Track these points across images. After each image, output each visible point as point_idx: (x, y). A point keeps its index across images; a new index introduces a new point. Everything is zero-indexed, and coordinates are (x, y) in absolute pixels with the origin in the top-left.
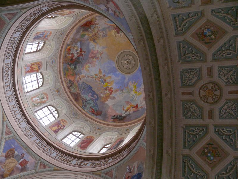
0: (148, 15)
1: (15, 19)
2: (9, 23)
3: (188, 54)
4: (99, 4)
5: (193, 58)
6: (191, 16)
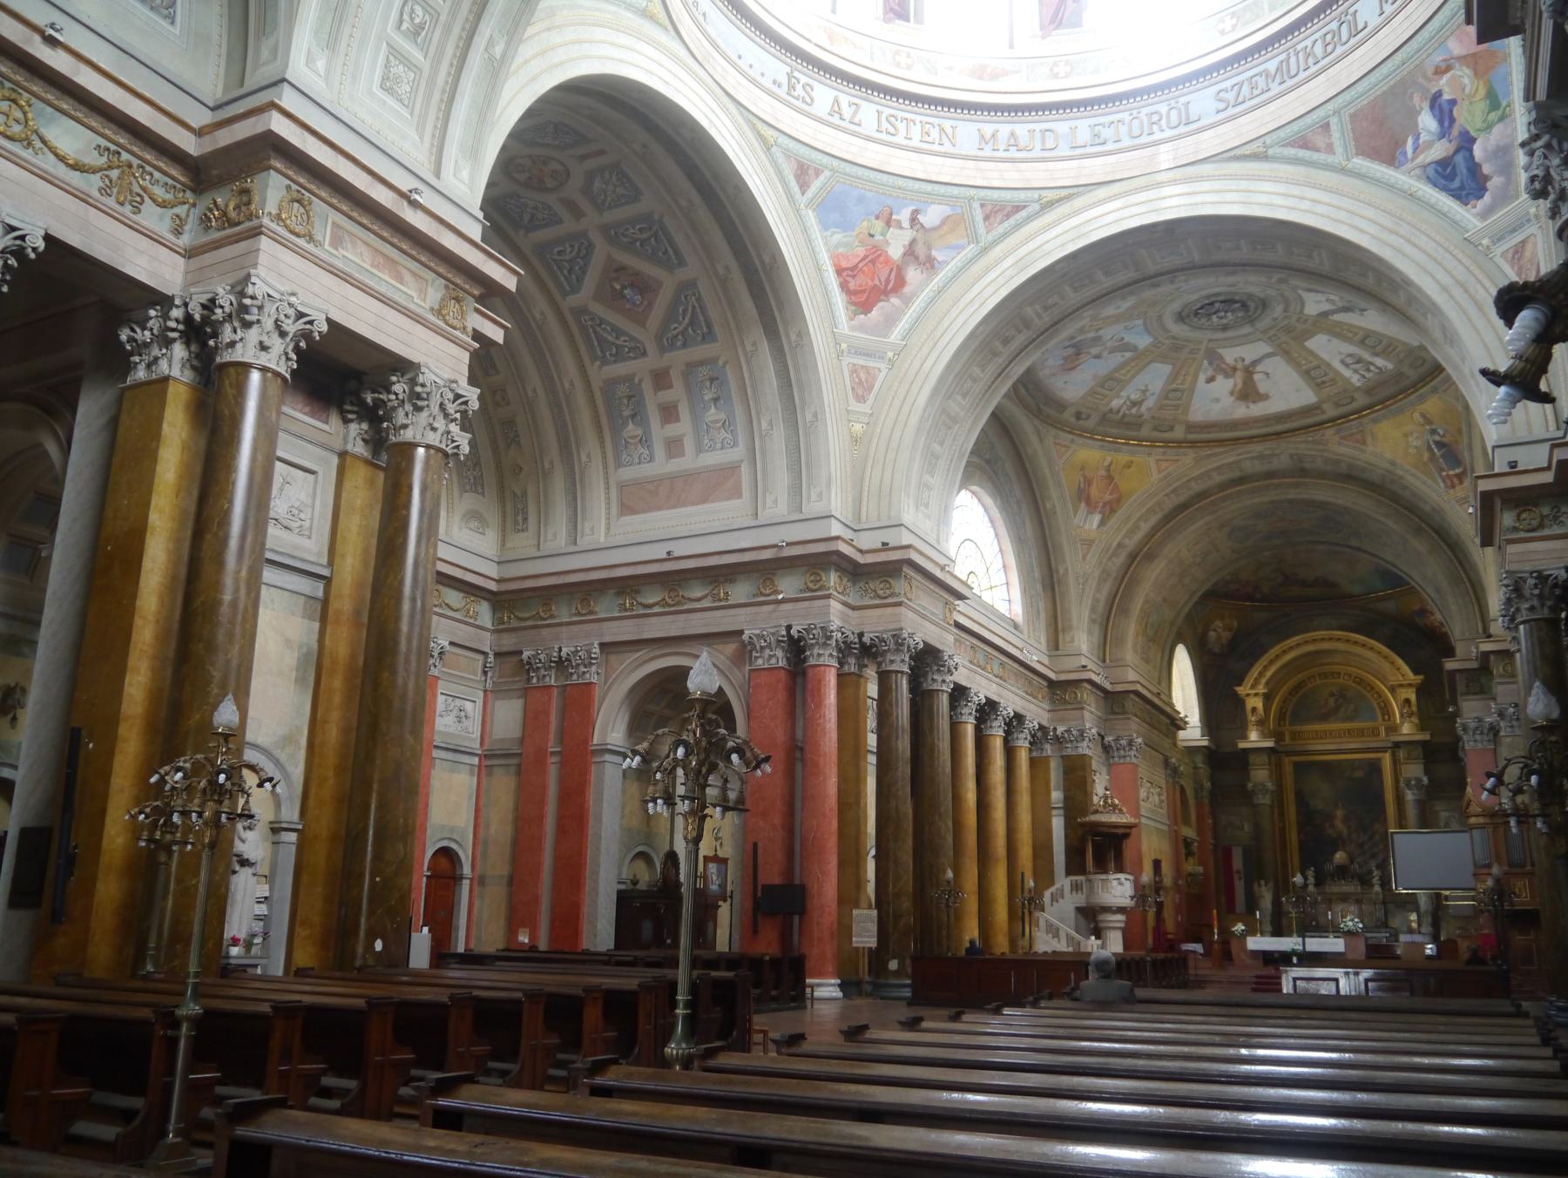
0: (765, 346)
1: (1308, 120)
2: (1337, 112)
3: (649, 238)
4: (943, 222)
5: (632, 231)
6: (680, 337)
